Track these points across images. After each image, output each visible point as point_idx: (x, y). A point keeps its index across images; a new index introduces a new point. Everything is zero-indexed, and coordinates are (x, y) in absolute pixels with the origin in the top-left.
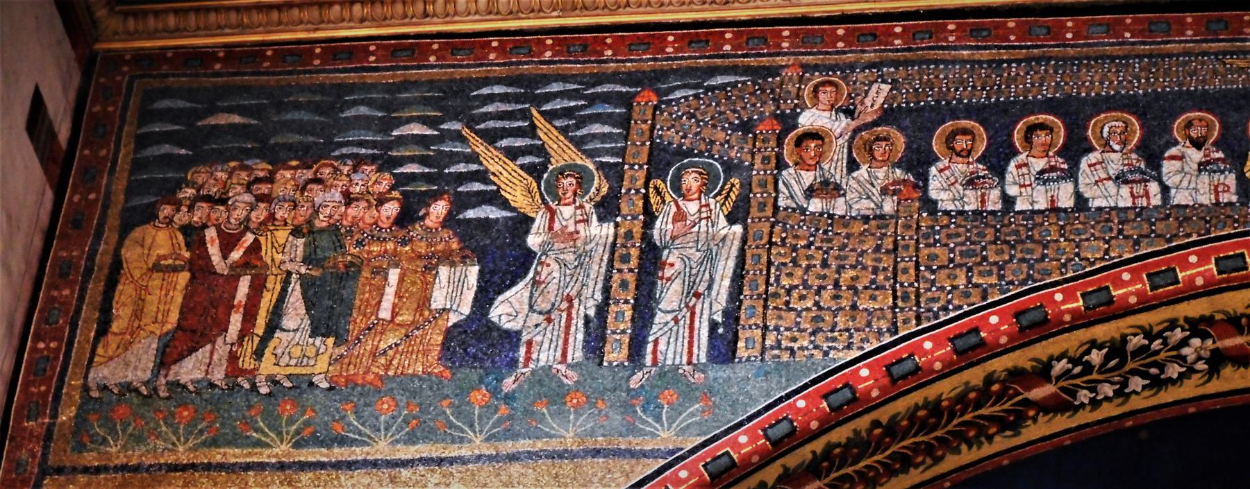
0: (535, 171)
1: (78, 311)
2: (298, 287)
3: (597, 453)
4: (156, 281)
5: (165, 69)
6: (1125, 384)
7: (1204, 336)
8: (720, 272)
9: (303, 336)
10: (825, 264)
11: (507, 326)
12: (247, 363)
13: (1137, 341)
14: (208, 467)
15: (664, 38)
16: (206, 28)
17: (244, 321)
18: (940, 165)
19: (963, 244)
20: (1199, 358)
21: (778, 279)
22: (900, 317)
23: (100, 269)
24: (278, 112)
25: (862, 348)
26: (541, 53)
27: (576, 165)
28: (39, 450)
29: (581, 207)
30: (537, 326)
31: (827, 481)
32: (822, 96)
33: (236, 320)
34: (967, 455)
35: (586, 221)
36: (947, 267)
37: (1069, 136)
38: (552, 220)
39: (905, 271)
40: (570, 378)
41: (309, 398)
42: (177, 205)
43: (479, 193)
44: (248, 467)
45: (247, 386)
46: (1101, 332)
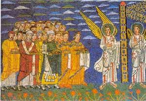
0: (100, 25)
4: (12, 56)
12: (38, 81)
24: (34, 6)
29: (112, 36)
30: (106, 71)
33: (34, 68)
35: (113, 41)
40: (115, 86)
41: (54, 90)
42: (14, 33)
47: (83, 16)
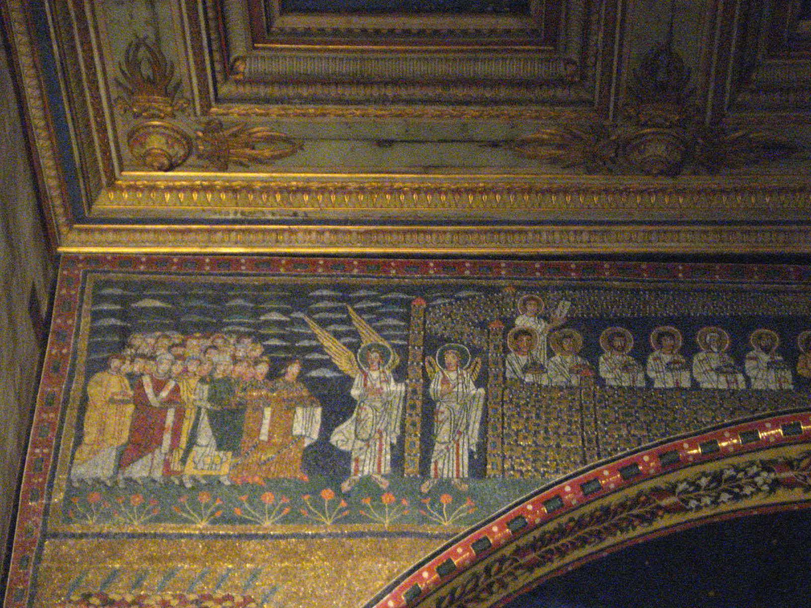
0: (353, 347)
1: (61, 428)
2: (206, 418)
3: (404, 534)
5: (107, 268)
6: (718, 497)
7: (769, 470)
8: (473, 419)
9: (212, 450)
10: (538, 416)
11: (343, 448)
12: (176, 466)
13: (730, 473)
14: (155, 535)
15: (427, 265)
16: (134, 241)
17: (172, 438)
18: (606, 356)
19: (624, 408)
20: (765, 483)
21: (509, 425)
22: (588, 454)
23: (74, 402)
25: (565, 473)
26: (352, 270)
27: (379, 345)
28: (40, 521)
29: (384, 372)
30: (361, 449)
31: (539, 553)
32: (529, 307)
33: (167, 439)
34: (620, 537)
36: (615, 423)
37: (685, 339)
38: (365, 379)
39: (589, 424)
40: (384, 484)
42: (123, 359)
43: (317, 360)
44: (182, 536)
45: (177, 482)
46: (711, 467)
47: (312, 324)
